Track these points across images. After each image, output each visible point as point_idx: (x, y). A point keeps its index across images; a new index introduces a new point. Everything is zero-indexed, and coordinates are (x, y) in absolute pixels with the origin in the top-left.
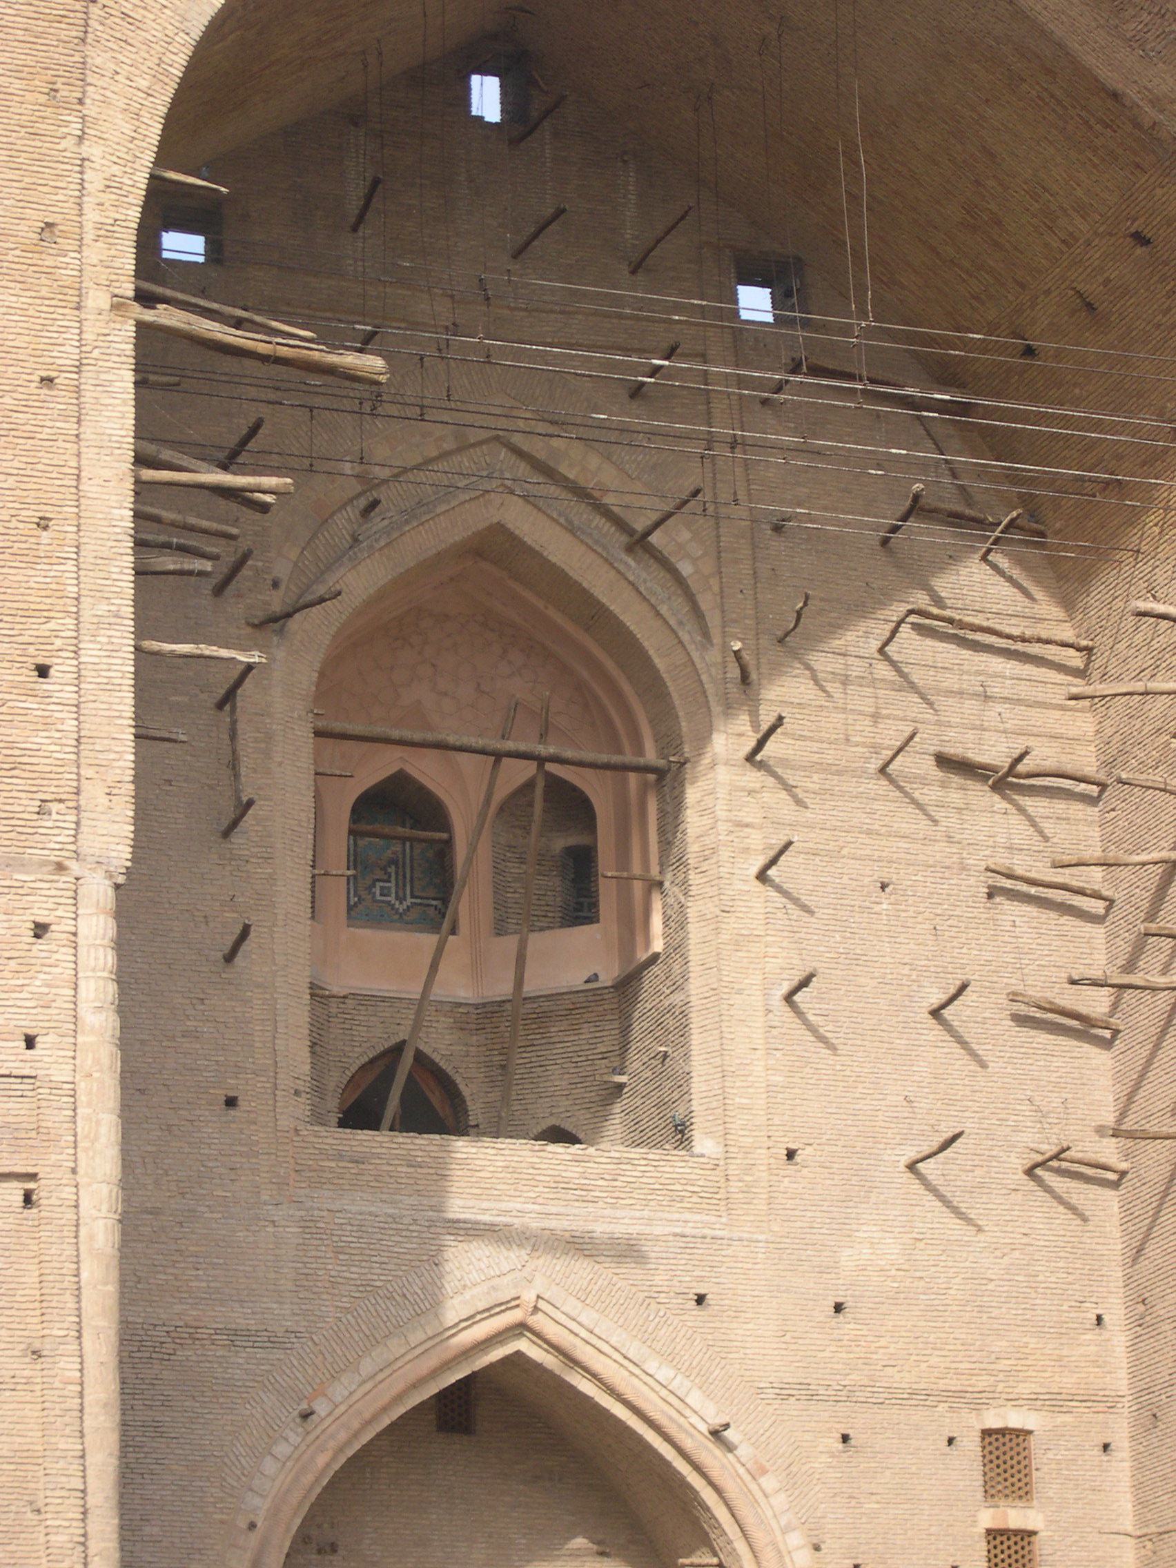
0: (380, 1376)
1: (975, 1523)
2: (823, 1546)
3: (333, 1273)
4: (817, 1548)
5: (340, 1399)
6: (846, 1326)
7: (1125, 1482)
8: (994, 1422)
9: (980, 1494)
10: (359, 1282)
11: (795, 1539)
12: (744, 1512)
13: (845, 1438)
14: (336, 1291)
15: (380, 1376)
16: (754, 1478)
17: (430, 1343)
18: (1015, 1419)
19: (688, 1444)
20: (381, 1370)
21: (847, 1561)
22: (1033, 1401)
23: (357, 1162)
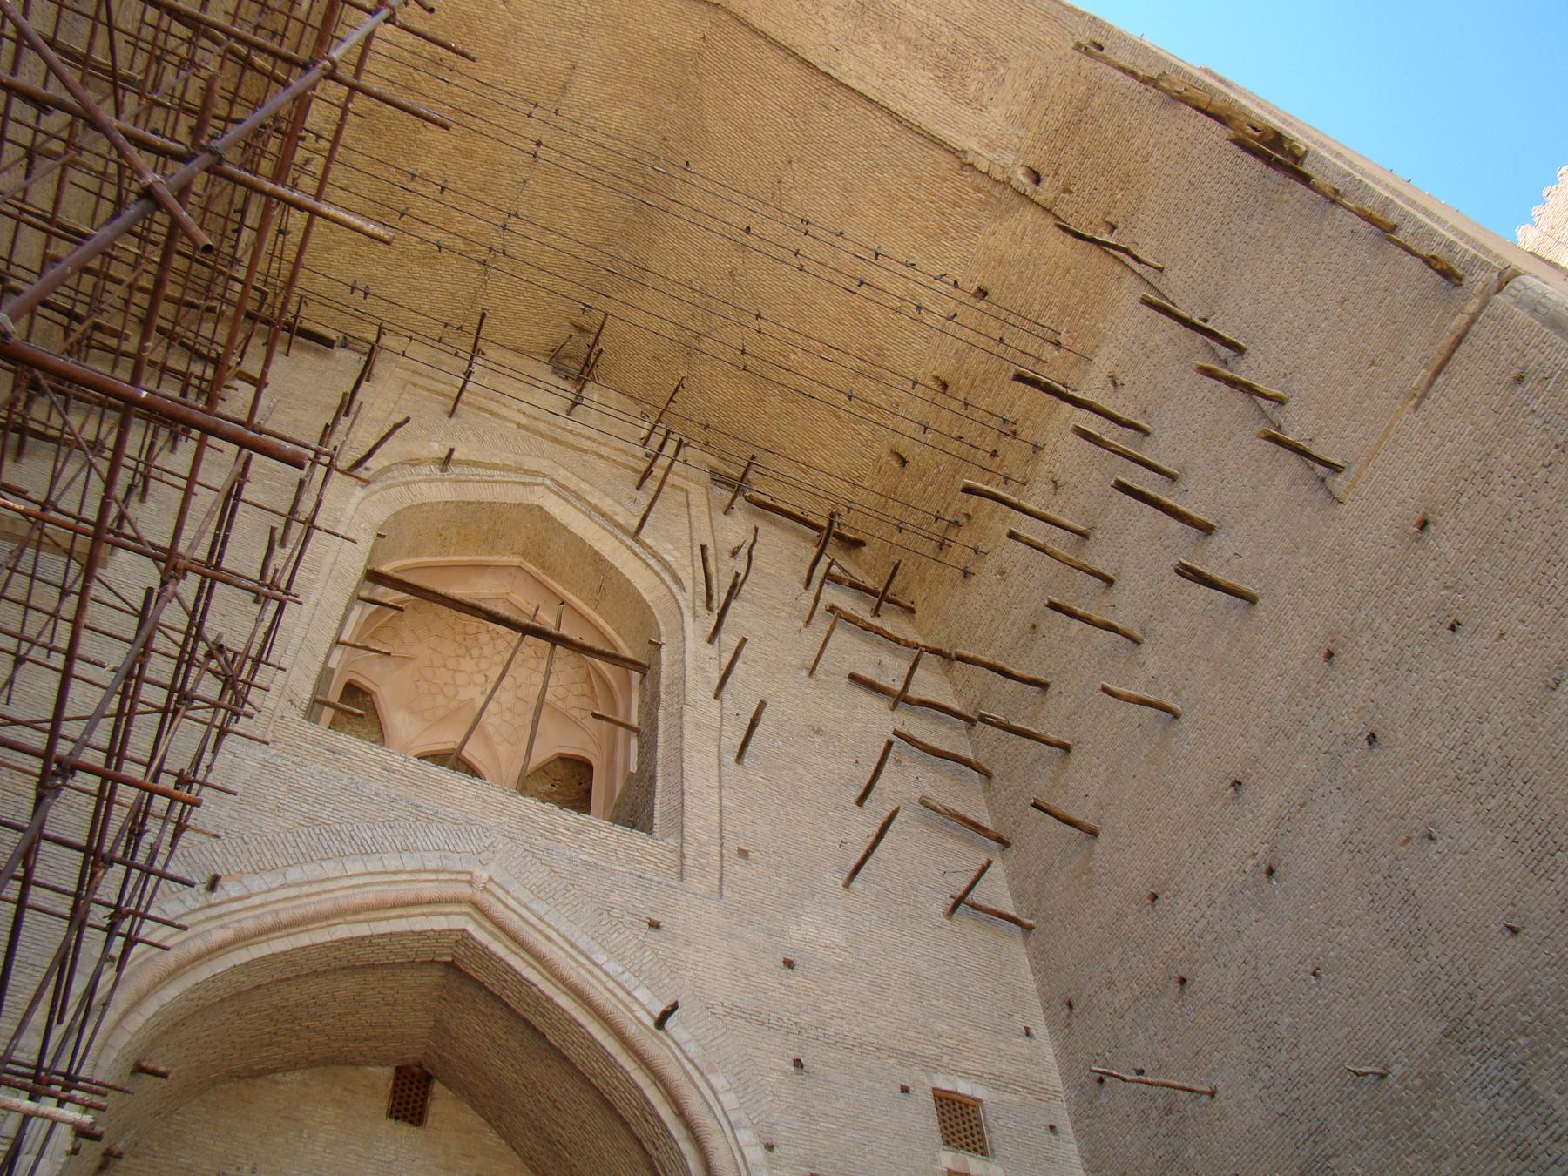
0: (306, 889)
1: (935, 1161)
2: (776, 1149)
3: (282, 801)
4: (770, 1147)
5: (255, 889)
6: (795, 979)
7: (1076, 1160)
8: (944, 1084)
9: (938, 1138)
10: (307, 815)
11: (745, 1136)
12: (694, 1105)
13: (798, 1063)
14: (281, 814)
15: (306, 889)
16: (702, 1074)
17: (368, 879)
18: (964, 1088)
19: (632, 1030)
20: (310, 883)
21: (805, 1169)
22: (980, 1078)
23: (334, 752)
